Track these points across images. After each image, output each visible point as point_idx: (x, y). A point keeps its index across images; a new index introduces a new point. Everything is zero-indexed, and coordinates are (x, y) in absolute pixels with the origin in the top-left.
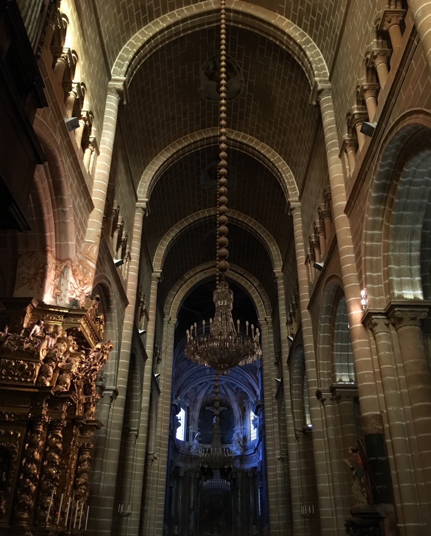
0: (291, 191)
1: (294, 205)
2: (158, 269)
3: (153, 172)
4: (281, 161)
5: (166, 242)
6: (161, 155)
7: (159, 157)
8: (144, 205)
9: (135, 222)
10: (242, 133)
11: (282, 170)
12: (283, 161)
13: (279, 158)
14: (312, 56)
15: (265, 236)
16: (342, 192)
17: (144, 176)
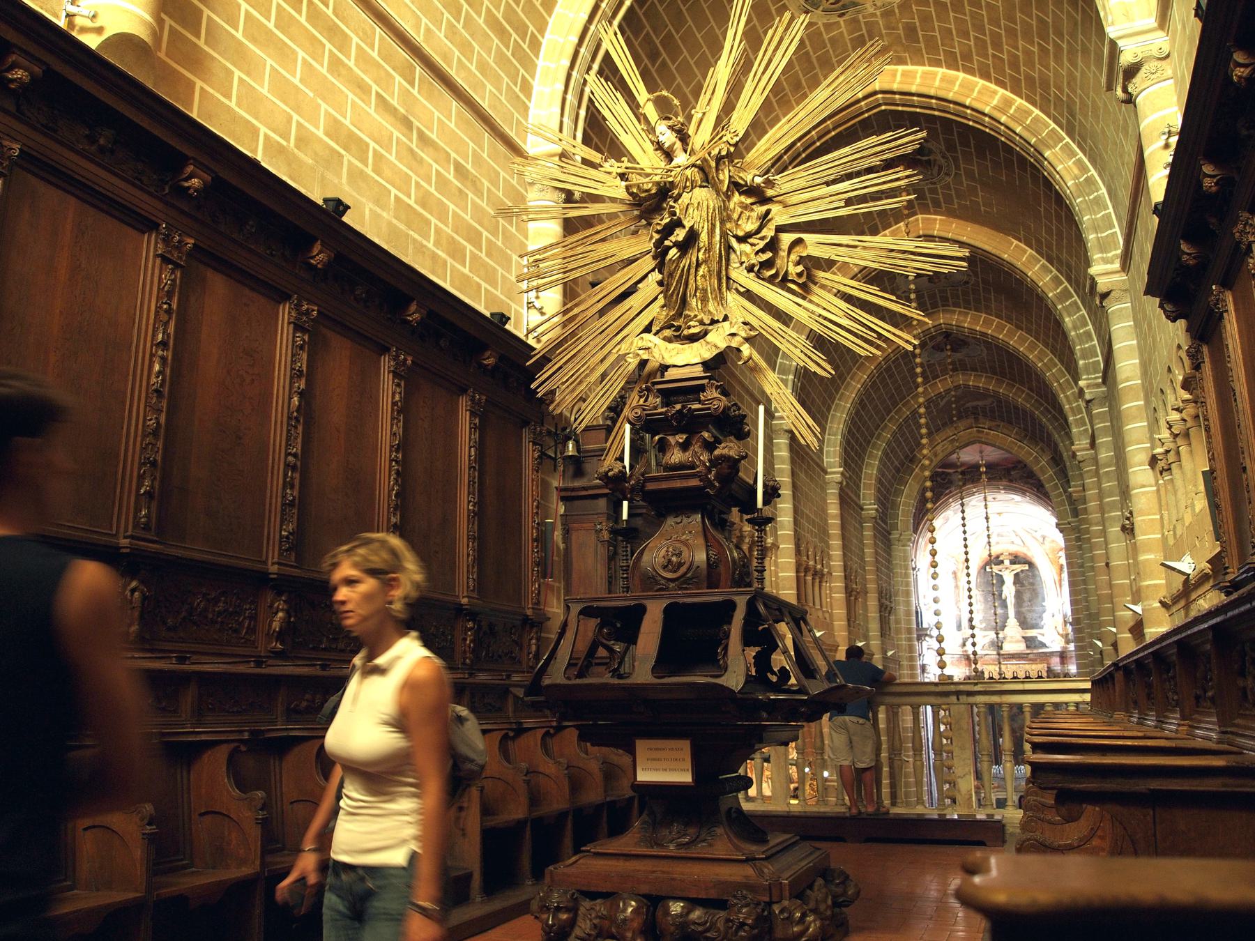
0: (1078, 427)
1: (1082, 456)
2: (870, 504)
3: (842, 413)
4: (1056, 365)
5: (878, 450)
6: (851, 379)
7: (849, 383)
8: (838, 477)
9: (830, 506)
10: (984, 315)
11: (1060, 384)
12: (1060, 365)
13: (1051, 360)
14: (1075, 328)
15: (1048, 420)
16: (1125, 596)
17: (831, 422)
